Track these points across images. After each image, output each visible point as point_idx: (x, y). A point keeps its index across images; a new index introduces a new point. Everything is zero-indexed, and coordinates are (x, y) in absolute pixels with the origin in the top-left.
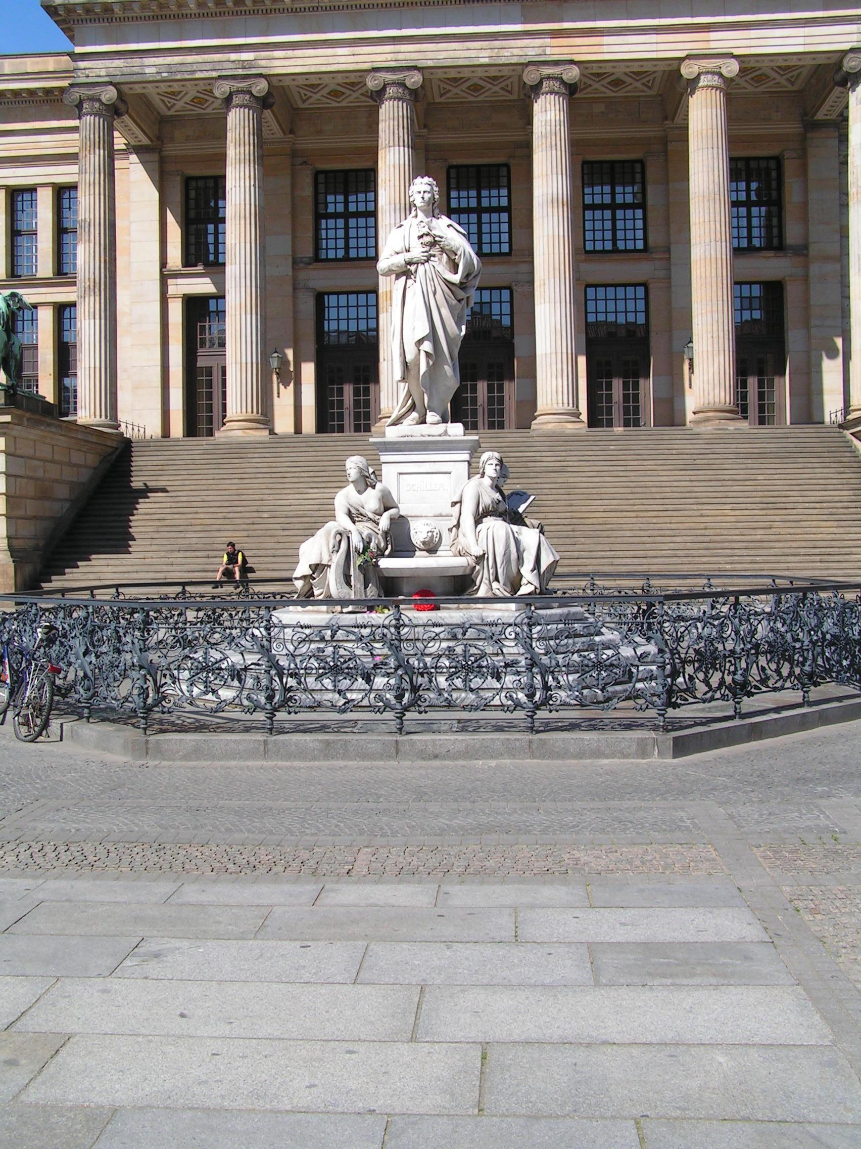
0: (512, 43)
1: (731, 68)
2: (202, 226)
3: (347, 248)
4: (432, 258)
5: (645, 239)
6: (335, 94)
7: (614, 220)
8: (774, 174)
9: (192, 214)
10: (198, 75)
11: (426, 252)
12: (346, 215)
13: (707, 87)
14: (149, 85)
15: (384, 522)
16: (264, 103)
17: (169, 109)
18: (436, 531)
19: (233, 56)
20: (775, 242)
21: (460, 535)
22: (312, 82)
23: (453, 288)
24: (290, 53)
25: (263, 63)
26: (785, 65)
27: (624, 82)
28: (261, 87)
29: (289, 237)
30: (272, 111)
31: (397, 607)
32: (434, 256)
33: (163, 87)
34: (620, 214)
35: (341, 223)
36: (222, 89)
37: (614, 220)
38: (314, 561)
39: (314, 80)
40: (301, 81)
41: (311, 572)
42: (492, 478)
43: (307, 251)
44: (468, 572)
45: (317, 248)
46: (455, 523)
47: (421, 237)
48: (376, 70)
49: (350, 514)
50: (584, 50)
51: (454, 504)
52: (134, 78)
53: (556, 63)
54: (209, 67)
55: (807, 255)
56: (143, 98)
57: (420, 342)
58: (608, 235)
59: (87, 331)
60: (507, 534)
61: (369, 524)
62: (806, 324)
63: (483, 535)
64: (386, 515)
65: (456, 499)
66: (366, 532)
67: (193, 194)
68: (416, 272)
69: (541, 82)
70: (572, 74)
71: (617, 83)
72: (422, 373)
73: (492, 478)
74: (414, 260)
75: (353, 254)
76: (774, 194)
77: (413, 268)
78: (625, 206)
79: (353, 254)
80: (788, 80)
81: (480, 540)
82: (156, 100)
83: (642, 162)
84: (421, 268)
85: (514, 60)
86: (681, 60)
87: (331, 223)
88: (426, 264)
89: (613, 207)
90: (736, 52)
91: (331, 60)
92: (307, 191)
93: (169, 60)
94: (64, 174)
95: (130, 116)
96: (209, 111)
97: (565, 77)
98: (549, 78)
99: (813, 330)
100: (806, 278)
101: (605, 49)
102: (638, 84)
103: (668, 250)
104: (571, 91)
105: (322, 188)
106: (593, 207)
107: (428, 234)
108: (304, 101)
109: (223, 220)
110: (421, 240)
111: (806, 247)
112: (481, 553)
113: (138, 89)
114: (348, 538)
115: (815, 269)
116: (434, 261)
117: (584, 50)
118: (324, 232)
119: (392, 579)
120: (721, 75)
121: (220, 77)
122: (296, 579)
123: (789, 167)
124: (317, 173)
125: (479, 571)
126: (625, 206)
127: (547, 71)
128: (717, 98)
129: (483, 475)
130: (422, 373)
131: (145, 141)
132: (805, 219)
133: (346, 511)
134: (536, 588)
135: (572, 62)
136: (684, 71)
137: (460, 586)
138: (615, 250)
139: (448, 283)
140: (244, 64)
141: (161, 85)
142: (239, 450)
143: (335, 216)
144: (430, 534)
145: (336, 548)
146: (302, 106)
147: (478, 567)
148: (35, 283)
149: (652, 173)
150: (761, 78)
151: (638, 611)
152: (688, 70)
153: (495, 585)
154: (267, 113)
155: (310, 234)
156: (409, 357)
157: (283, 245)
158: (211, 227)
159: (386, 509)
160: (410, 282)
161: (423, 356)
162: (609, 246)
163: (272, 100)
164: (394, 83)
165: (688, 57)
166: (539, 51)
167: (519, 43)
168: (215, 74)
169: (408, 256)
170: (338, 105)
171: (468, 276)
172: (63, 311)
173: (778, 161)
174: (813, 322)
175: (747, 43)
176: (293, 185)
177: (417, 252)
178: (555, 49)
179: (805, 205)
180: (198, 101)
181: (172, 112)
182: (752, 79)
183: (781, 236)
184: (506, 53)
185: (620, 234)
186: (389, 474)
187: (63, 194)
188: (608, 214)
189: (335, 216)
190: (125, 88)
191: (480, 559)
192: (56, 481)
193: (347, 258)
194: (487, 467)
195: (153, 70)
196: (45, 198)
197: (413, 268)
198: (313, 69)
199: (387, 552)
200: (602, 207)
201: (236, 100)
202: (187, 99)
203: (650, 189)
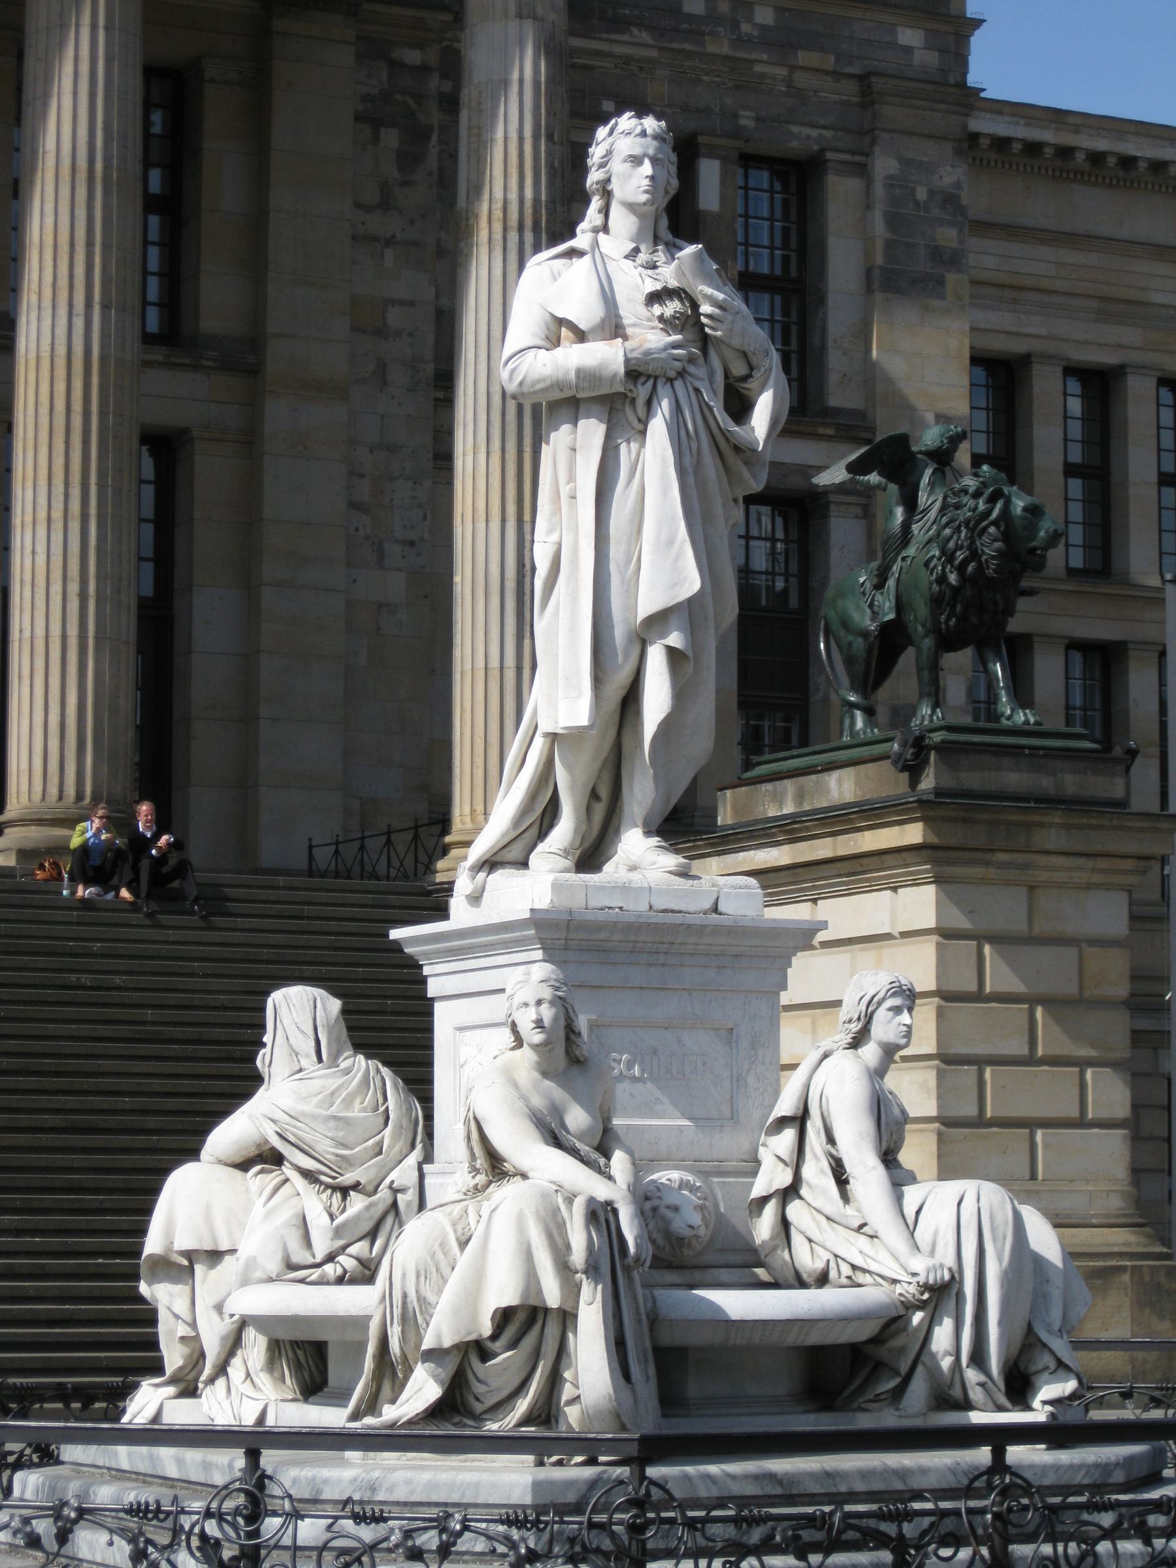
4: (692, 369)
47: (654, 298)
57: (658, 621)
62: (247, 577)
68: (649, 403)
88: (678, 384)
99: (268, 596)
100: (250, 441)
110: (657, 310)
115: (278, 413)
119: (681, 1352)
137: (850, 1372)
147: (917, 1317)
179: (257, 222)
194: (881, 1015)
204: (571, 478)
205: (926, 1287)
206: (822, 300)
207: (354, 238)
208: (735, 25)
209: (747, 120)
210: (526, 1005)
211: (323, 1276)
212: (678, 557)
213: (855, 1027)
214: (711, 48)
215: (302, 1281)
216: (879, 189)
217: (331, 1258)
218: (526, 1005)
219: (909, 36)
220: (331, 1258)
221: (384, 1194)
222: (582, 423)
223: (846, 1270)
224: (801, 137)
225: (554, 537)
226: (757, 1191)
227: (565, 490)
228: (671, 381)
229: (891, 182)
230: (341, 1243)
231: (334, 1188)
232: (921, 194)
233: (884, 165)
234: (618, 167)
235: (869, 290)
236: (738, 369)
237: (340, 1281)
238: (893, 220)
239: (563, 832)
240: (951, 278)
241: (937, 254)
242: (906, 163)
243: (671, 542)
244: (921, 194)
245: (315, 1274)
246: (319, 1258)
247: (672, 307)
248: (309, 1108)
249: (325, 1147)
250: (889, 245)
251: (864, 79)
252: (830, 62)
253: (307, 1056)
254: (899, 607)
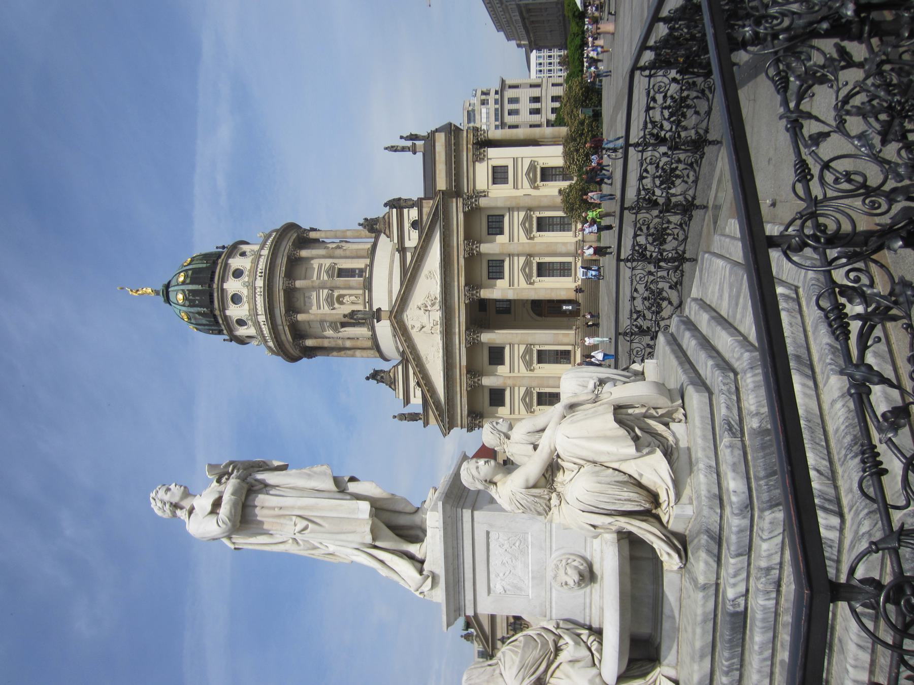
47: (219, 481)
68: (257, 480)
194: (498, 427)
204: (273, 508)
210: (477, 468)
211: (597, 650)
212: (315, 473)
213: (502, 436)
215: (600, 661)
217: (590, 649)
218: (477, 468)
220: (590, 649)
221: (559, 631)
222: (256, 503)
225: (294, 518)
227: (277, 512)
230: (582, 643)
231: (556, 655)
234: (167, 498)
237: (601, 643)
239: (413, 549)
243: (309, 475)
245: (596, 654)
246: (588, 653)
248: (517, 660)
249: (536, 653)
253: (494, 670)
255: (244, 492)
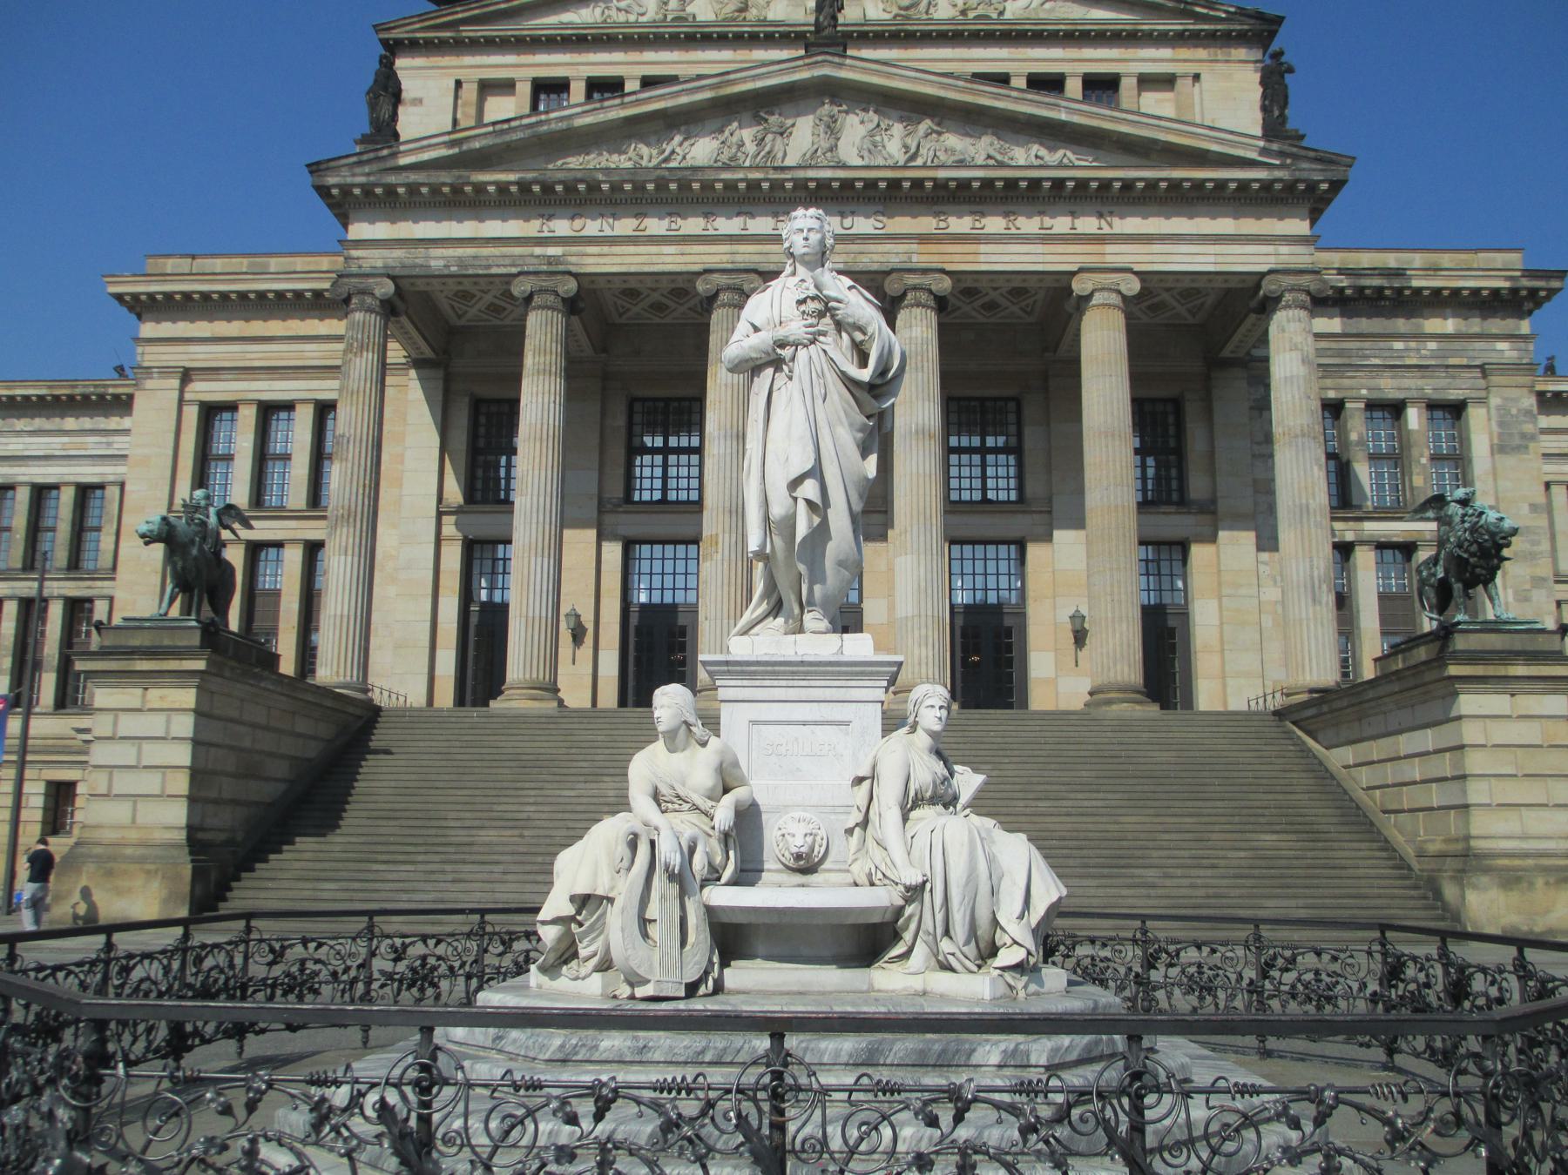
0: (872, 248)
1: (1133, 286)
2: (491, 458)
3: (665, 489)
5: (1020, 488)
6: (658, 307)
7: (984, 466)
8: (1171, 419)
9: (481, 443)
10: (494, 271)
11: (811, 326)
12: (666, 451)
13: (1103, 305)
14: (434, 281)
15: (724, 814)
16: (571, 306)
17: (460, 317)
18: (822, 833)
19: (538, 251)
20: (1175, 496)
21: (870, 843)
22: (631, 287)
23: (858, 393)
24: (606, 249)
25: (573, 259)
26: (1189, 286)
27: (998, 306)
28: (571, 286)
29: (596, 475)
30: (581, 319)
31: (777, 1037)
32: (824, 334)
33: (452, 286)
34: (990, 458)
35: (658, 459)
36: (520, 288)
37: (984, 466)
38: (581, 889)
39: (633, 284)
40: (618, 284)
41: (569, 910)
42: (933, 735)
43: (619, 493)
44: (888, 917)
45: (629, 488)
46: (859, 817)
47: (801, 302)
48: (707, 271)
49: (656, 796)
50: (957, 258)
51: (859, 781)
52: (417, 271)
53: (925, 271)
54: (507, 262)
55: (1214, 513)
56: (426, 298)
57: (795, 484)
58: (977, 483)
59: (338, 570)
60: (972, 842)
61: (694, 817)
63: (921, 843)
64: (728, 800)
65: (864, 771)
66: (687, 833)
67: (483, 420)
68: (793, 359)
69: (904, 294)
70: (946, 284)
71: (991, 306)
72: (798, 539)
73: (933, 735)
74: (791, 339)
75: (672, 496)
76: (1172, 443)
77: (786, 353)
78: (996, 451)
79: (672, 496)
80: (1189, 311)
81: (915, 853)
82: (445, 305)
83: (1018, 401)
84: (802, 354)
85: (875, 267)
86: (1073, 274)
87: (647, 459)
89: (983, 451)
90: (1137, 268)
91: (655, 259)
92: (620, 421)
93: (460, 252)
94: (325, 389)
95: (410, 318)
96: (507, 322)
97: (933, 288)
98: (915, 288)
101: (982, 258)
102: (1015, 309)
103: (1050, 500)
104: (941, 304)
105: (637, 418)
106: (959, 450)
107: (813, 299)
108: (621, 315)
109: (514, 451)
110: (803, 308)
111: (1214, 501)
112: (920, 880)
113: (421, 285)
114: (652, 843)
116: (828, 342)
117: (957, 258)
118: (638, 470)
120: (1119, 292)
121: (520, 274)
122: (544, 923)
123: (1192, 410)
124: (632, 401)
125: (910, 917)
126: (996, 451)
127: (912, 280)
128: (1118, 319)
129: (914, 729)
130: (798, 539)
131: (428, 353)
132: (1212, 471)
133: (650, 790)
134: (1029, 953)
135: (943, 271)
136: (1075, 286)
138: (985, 500)
139: (850, 383)
140: (550, 260)
141: (450, 281)
142: (518, 721)
143: (653, 451)
144: (809, 839)
145: (626, 863)
146: (618, 321)
147: (909, 910)
148: (281, 513)
149: (1029, 411)
150: (1156, 308)
151: (1127, 975)
152: (1079, 286)
153: (945, 946)
154: (575, 319)
155: (621, 471)
156: (777, 511)
157: (589, 482)
158: (504, 459)
159: (726, 791)
160: (781, 378)
161: (802, 505)
162: (977, 496)
163: (582, 305)
164: (729, 288)
165: (1081, 270)
166: (904, 258)
167: (880, 248)
168: (514, 270)
169: (781, 333)
170: (657, 320)
171: (884, 373)
172: (313, 549)
173: (1177, 404)
174: (1225, 591)
175: (1149, 258)
176: (603, 414)
177: (796, 328)
178: (922, 256)
179: (1211, 455)
180: (494, 309)
181: (463, 322)
182: (1149, 308)
183: (1182, 489)
184: (865, 259)
185: (991, 483)
186: (733, 718)
187: (324, 409)
188: (976, 458)
189: (653, 451)
190: (404, 283)
191: (915, 892)
192: (271, 755)
193: (664, 501)
194: (923, 711)
195: (442, 263)
196: (303, 419)
197: (786, 353)
198: (633, 269)
199: (727, 875)
200: (970, 450)
201: (537, 300)
202: (482, 305)
203: (1028, 431)
205: (908, 889)
206: (1470, 461)
207: (1254, 456)
208: (1418, 350)
209: (1429, 392)
214: (1408, 362)
216: (1493, 412)
219: (1502, 346)
223: (880, 875)
224: (1454, 395)
226: (851, 825)
228: (806, 346)
229: (1498, 408)
232: (1514, 411)
233: (1494, 401)
235: (1492, 454)
236: (859, 336)
238: (1501, 424)
240: (1532, 445)
241: (1523, 436)
242: (1506, 399)
244: (1514, 411)
247: (812, 306)
250: (1500, 435)
251: (1481, 367)
252: (1465, 362)
254: (1446, 571)
255: (766, 359)
